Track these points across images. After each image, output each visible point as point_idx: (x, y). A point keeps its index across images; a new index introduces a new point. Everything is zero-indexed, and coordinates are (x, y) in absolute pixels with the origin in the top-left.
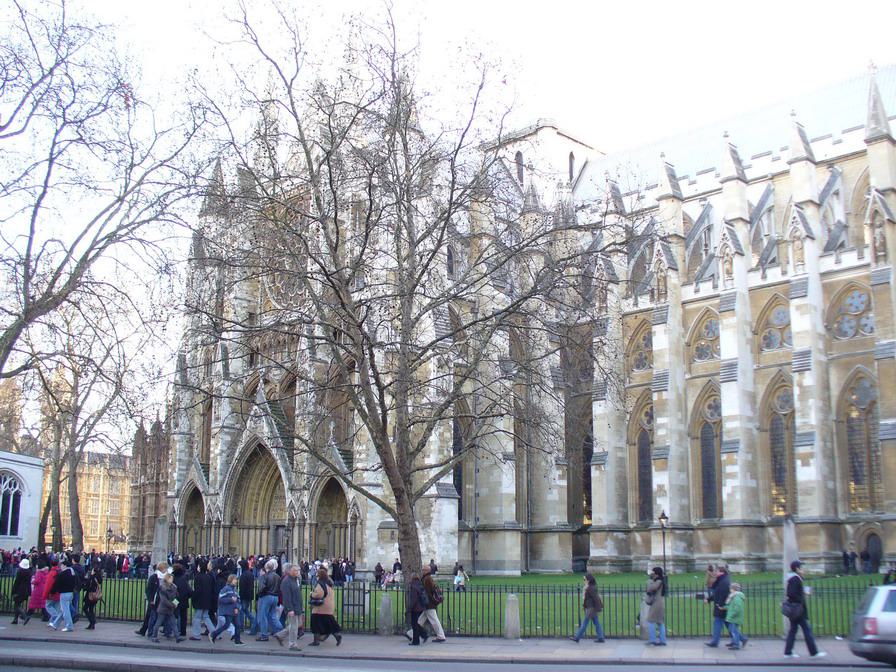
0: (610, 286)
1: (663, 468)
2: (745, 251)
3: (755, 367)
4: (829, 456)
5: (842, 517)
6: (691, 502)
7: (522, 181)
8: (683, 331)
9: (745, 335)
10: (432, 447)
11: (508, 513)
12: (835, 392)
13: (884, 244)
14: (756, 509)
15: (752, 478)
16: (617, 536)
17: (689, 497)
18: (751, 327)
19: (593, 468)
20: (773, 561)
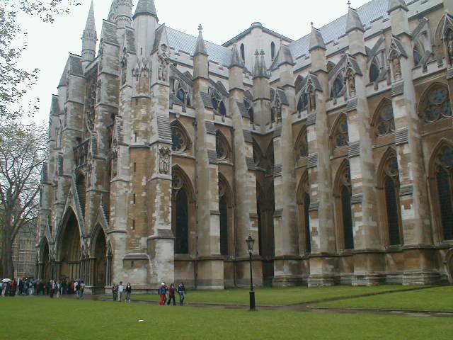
0: (283, 106)
1: (316, 217)
2: (363, 73)
3: (373, 147)
4: (424, 202)
5: (437, 244)
7: (244, 59)
8: (327, 129)
10: (156, 206)
11: (215, 249)
12: (427, 158)
14: (377, 241)
15: (373, 220)
16: (291, 263)
18: (369, 122)
19: (275, 220)
20: (391, 277)
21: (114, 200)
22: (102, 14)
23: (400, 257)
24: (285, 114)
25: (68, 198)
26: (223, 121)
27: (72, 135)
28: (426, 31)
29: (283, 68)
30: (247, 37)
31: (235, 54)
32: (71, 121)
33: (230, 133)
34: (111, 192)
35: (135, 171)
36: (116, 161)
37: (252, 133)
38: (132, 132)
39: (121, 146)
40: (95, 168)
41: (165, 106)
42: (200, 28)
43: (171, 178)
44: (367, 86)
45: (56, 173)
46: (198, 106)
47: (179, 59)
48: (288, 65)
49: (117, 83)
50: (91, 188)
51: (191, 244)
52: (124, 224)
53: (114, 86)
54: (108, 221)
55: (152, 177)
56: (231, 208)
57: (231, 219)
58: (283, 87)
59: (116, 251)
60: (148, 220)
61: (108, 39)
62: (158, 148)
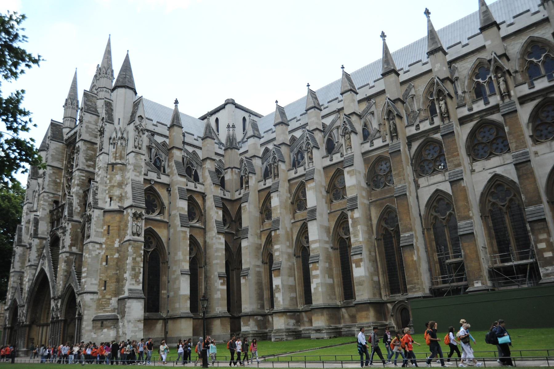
0: (250, 175)
1: (278, 275)
2: (320, 146)
3: (329, 212)
4: (374, 261)
5: (385, 299)
6: (298, 294)
7: (218, 132)
8: (289, 195)
9: (321, 193)
10: (128, 267)
11: (184, 307)
12: (375, 221)
13: (395, 129)
14: (333, 297)
15: (329, 277)
17: (296, 292)
18: (325, 188)
19: (242, 278)
20: (346, 329)
21: (86, 262)
23: (353, 310)
24: (253, 181)
25: (41, 260)
26: (196, 187)
27: (49, 198)
28: (373, 112)
29: (251, 141)
30: (221, 111)
31: (208, 127)
32: (48, 185)
33: (201, 199)
34: (84, 254)
35: (108, 233)
36: (90, 224)
37: (222, 198)
38: (107, 196)
39: (95, 210)
40: (69, 231)
41: (140, 173)
42: (176, 102)
44: (323, 158)
45: (31, 234)
46: (172, 172)
47: (157, 130)
48: (256, 139)
49: (95, 150)
50: (64, 250)
51: (162, 302)
53: (93, 153)
55: (125, 239)
56: (202, 267)
58: (251, 157)
59: (86, 312)
60: (119, 280)
62: (131, 211)
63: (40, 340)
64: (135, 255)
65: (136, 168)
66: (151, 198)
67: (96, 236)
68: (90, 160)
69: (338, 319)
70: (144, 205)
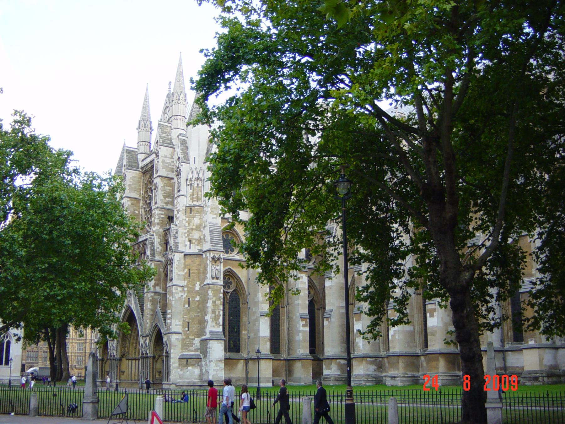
11: (265, 348)
19: (325, 319)
22: (156, 117)
34: (168, 296)
35: (189, 276)
36: (172, 267)
38: (187, 239)
39: (176, 254)
43: (222, 283)
49: (172, 186)
52: (180, 325)
53: (170, 188)
54: (165, 323)
55: (205, 283)
57: (284, 318)
59: (172, 351)
60: (202, 322)
61: (163, 142)
63: (130, 373)
64: (214, 298)
65: (213, 210)
66: (230, 236)
67: (178, 279)
68: (168, 196)
69: (417, 367)
70: (222, 248)
